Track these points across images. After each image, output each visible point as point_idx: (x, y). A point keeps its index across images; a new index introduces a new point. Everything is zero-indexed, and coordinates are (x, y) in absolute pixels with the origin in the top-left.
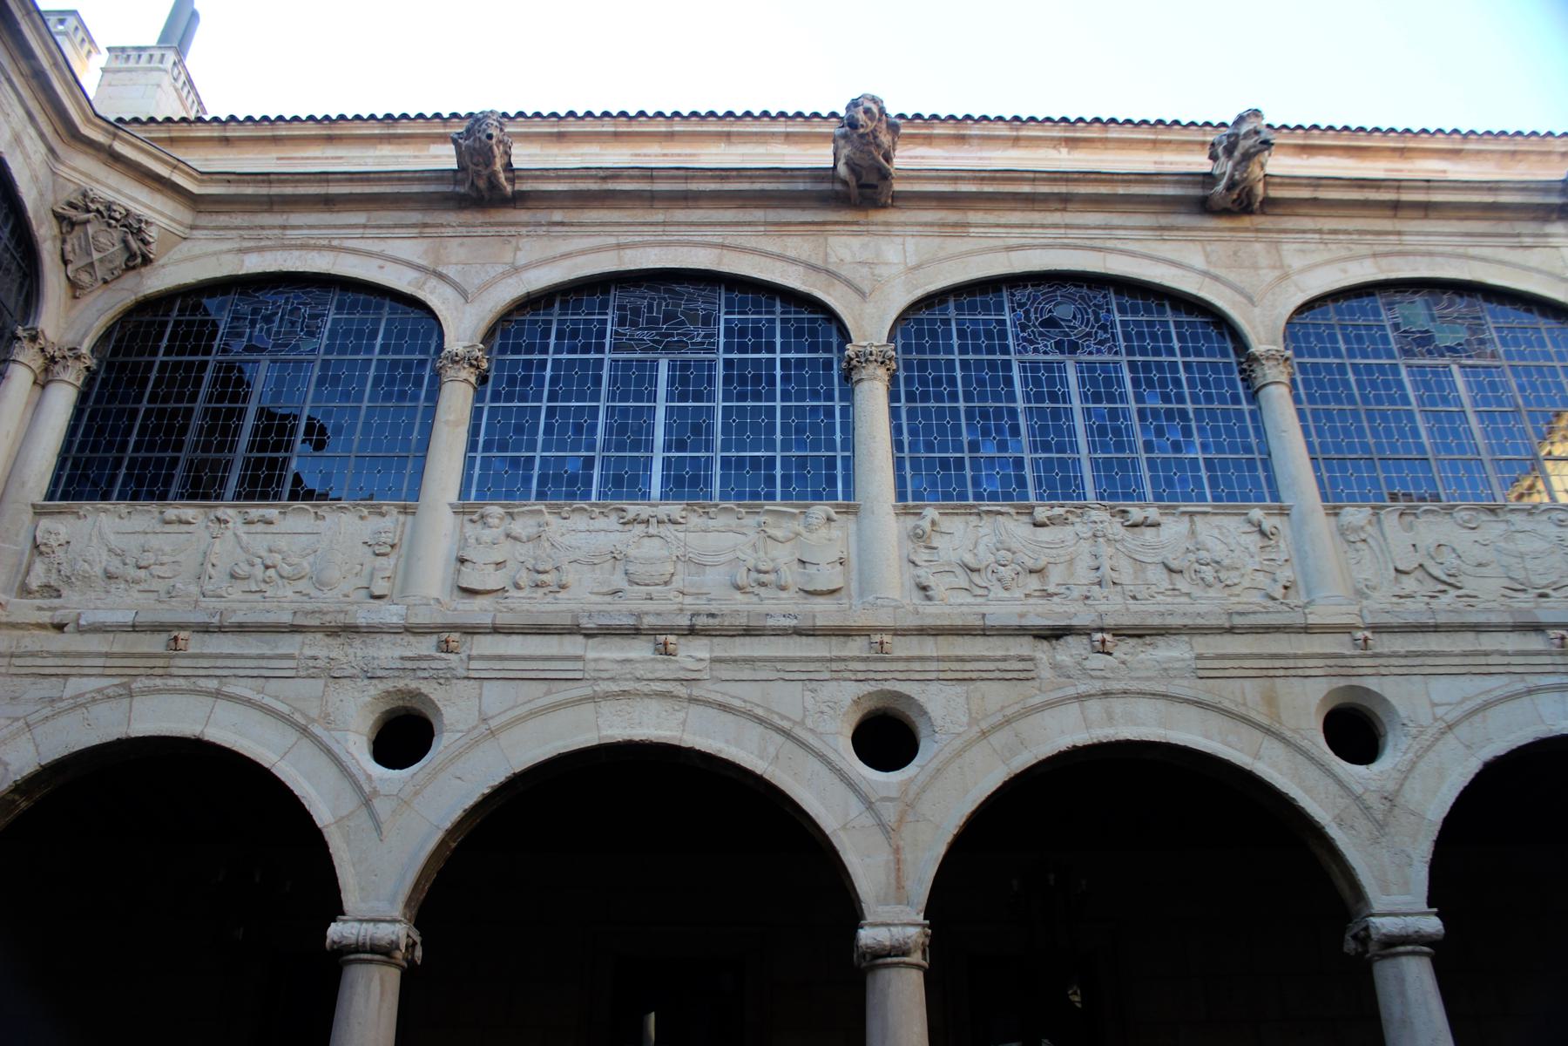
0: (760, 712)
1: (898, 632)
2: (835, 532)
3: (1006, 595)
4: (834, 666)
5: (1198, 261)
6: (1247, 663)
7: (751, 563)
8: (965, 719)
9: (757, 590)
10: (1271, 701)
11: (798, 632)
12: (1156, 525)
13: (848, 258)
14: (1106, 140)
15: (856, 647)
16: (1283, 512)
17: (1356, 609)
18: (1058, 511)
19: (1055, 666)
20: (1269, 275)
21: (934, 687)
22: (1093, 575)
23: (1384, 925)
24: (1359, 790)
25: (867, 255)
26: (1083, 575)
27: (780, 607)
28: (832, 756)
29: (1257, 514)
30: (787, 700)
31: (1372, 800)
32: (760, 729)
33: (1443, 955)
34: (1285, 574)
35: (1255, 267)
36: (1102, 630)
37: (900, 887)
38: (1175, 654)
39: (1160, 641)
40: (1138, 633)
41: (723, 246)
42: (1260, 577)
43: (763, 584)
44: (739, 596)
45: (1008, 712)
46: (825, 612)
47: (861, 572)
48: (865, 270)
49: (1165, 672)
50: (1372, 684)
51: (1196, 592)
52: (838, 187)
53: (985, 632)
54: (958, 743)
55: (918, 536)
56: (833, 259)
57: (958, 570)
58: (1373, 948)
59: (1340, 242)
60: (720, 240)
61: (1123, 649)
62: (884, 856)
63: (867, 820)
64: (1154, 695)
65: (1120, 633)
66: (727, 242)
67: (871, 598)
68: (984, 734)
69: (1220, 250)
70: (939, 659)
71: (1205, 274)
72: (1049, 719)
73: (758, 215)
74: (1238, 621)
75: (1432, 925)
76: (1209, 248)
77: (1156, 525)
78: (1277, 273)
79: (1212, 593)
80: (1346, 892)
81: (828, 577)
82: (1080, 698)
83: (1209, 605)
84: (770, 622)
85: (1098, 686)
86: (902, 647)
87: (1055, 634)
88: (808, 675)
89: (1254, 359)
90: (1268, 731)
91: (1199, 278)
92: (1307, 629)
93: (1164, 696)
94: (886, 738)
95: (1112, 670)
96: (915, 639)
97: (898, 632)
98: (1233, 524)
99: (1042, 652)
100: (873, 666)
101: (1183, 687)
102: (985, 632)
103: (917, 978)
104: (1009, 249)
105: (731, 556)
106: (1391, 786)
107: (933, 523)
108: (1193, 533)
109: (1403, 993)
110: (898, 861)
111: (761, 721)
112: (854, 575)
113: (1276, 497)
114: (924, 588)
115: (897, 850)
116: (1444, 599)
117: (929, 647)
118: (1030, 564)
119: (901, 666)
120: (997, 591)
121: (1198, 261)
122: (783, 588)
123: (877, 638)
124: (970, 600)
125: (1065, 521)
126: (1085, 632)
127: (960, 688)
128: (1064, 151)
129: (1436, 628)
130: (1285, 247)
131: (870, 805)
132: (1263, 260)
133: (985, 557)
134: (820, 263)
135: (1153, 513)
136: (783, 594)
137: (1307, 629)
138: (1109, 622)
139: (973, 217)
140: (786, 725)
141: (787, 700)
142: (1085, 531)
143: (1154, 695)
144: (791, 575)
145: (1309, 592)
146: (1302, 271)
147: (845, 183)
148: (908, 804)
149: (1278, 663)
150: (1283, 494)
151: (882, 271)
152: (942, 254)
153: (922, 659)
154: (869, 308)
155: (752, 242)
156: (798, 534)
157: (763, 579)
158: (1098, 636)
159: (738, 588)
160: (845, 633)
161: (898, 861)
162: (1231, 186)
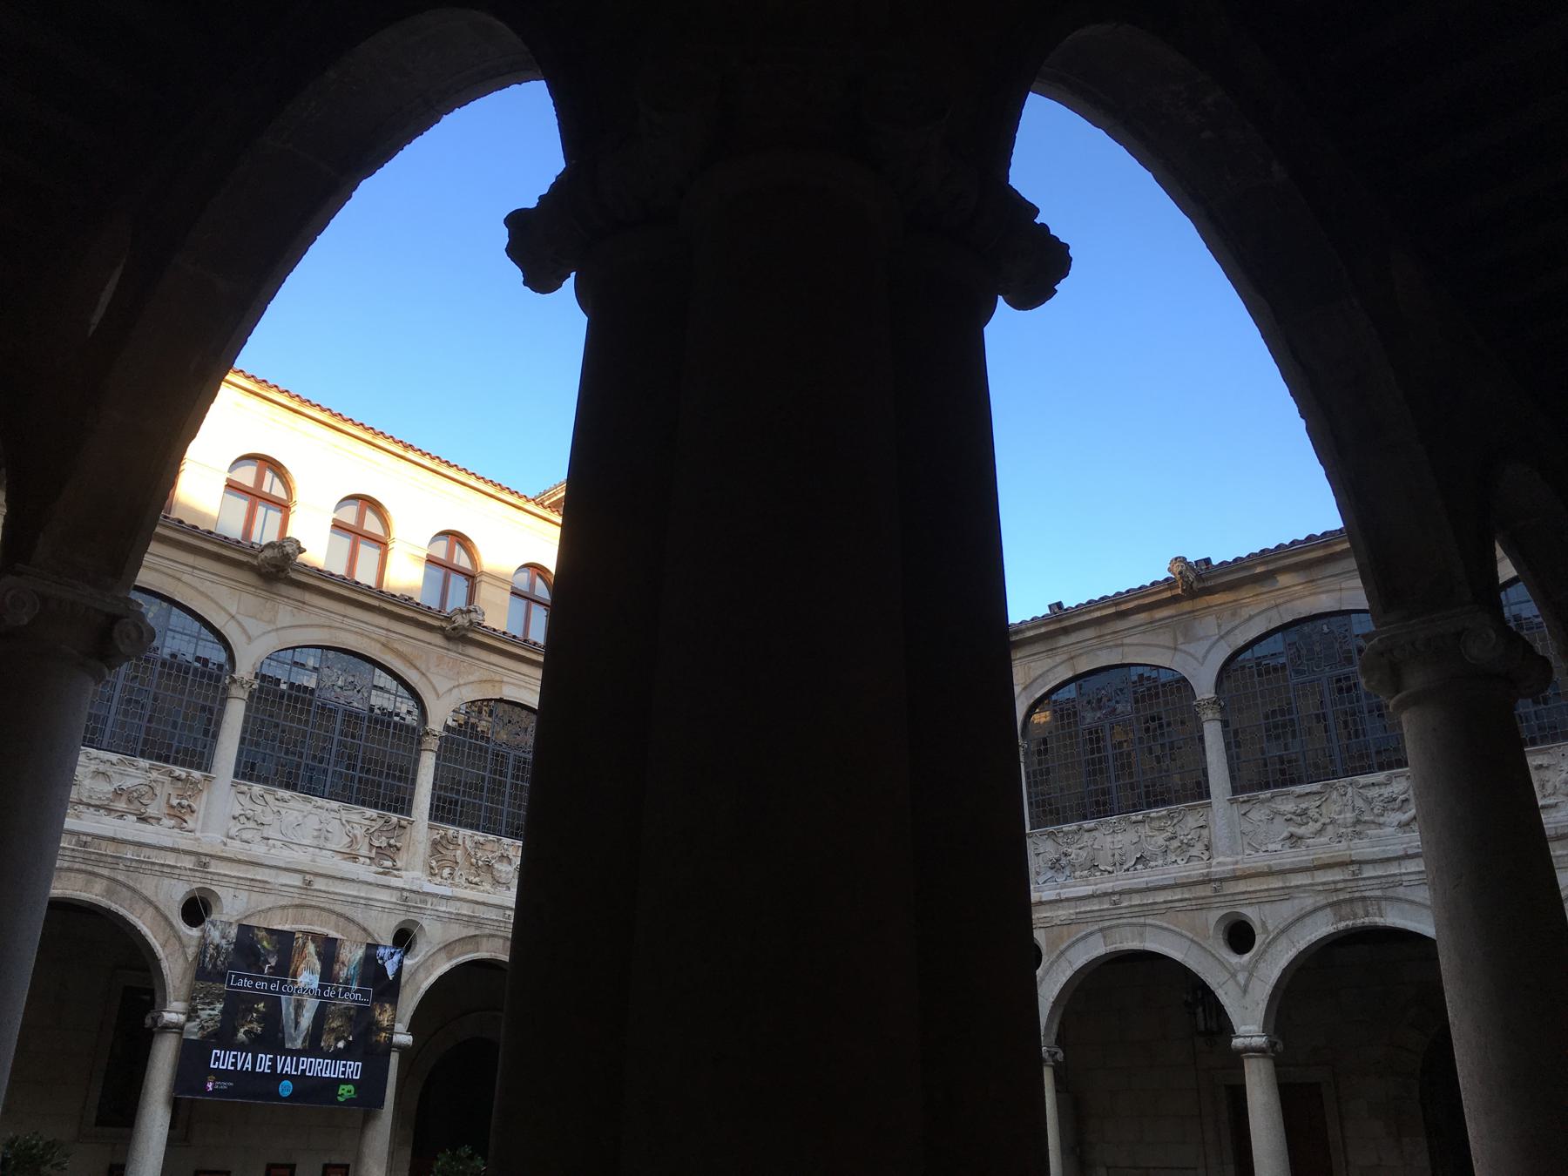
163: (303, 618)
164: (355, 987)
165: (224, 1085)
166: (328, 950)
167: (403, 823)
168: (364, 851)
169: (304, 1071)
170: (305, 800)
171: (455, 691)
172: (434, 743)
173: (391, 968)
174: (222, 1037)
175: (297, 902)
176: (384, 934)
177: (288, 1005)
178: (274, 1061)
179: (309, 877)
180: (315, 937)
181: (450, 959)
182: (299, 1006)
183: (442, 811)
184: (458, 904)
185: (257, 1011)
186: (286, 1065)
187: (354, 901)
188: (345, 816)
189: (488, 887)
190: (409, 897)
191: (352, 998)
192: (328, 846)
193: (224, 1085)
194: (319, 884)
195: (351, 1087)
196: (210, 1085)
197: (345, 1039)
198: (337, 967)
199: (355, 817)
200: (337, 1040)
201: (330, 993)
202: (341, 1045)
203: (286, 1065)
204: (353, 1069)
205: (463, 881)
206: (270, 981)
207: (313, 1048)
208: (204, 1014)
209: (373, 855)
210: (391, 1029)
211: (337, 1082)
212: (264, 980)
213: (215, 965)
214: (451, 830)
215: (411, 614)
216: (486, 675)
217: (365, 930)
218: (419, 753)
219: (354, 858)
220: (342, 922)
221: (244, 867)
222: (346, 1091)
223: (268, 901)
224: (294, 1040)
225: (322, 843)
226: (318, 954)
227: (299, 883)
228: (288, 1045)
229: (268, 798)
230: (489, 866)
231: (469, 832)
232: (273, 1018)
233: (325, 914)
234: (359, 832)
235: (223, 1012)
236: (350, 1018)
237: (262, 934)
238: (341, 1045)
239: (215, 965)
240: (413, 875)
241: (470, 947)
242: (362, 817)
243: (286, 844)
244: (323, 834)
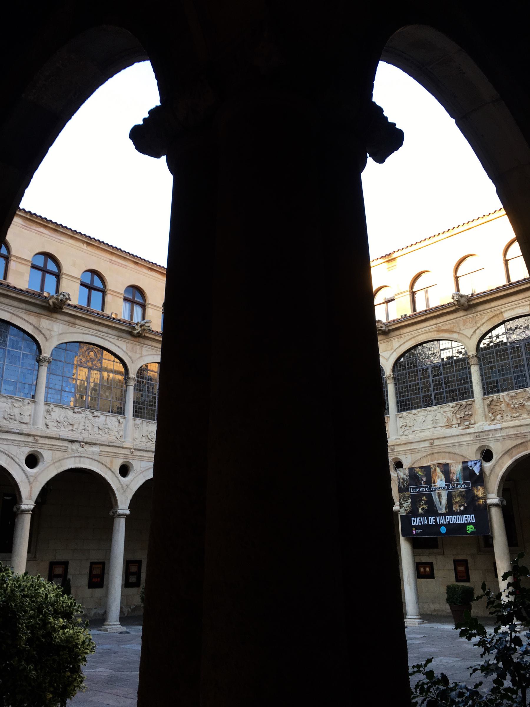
0: (7, 452)
1: (41, 437)
2: (29, 407)
3: (64, 429)
4: (25, 443)
5: (124, 348)
6: (109, 454)
7: (9, 413)
8: (51, 459)
9: (9, 420)
10: (111, 462)
11: (19, 434)
12: (99, 417)
13: (45, 327)
14: (99, 247)
15: (31, 439)
16: (125, 418)
17: (132, 444)
18: (80, 410)
19: (72, 449)
20: (138, 356)
21: (45, 451)
22: (83, 427)
23: (120, 512)
24: (122, 483)
25: (50, 327)
26: (82, 427)
27: (14, 426)
28: (21, 464)
29: (119, 418)
30: (13, 450)
31: (124, 486)
32: (6, 456)
33: (128, 519)
34: (121, 433)
35: (136, 353)
36: (83, 442)
37: (30, 496)
38: (96, 449)
39: (94, 446)
40: (90, 444)
41: (12, 313)
42: (116, 433)
43: (11, 419)
44: (5, 421)
45: (60, 458)
46: (25, 429)
47: (34, 419)
48: (48, 332)
49: (93, 453)
50: (131, 461)
51: (103, 435)
52: (47, 305)
53: (59, 439)
54: (48, 464)
55: (48, 411)
56: (41, 326)
57: (55, 422)
58: (116, 515)
59: (155, 350)
60: (12, 311)
61: (86, 447)
62: (28, 488)
63: (26, 480)
64: (90, 458)
65: (87, 443)
66: (14, 313)
67: (36, 427)
68: (54, 463)
69: (130, 345)
70: (48, 444)
71: (125, 352)
72: (68, 461)
73: (23, 306)
74: (110, 444)
75: (128, 512)
76: (128, 345)
77: (99, 417)
78: (140, 355)
79: (106, 435)
80: (114, 503)
81: (26, 419)
82: (75, 457)
83: (104, 438)
84: (13, 431)
85: (79, 455)
86: (41, 441)
87: (73, 442)
88: (19, 444)
89: (129, 378)
90: (109, 469)
91: (123, 352)
92: (122, 448)
93: (92, 459)
94: (32, 461)
95: (83, 451)
96: (44, 439)
97: (41, 437)
98: (114, 419)
99: (69, 445)
100: (34, 444)
101: (96, 457)
102: (59, 439)
103: (30, 516)
104: (83, 333)
105: (4, 410)
106: (128, 483)
107: (52, 409)
108: (106, 420)
109: (119, 525)
110: (31, 490)
111: (6, 454)
112: (32, 419)
113: (124, 414)
114: (47, 425)
115: (31, 488)
116: (149, 444)
117: (47, 441)
118: (71, 423)
119: (40, 445)
120: (63, 429)
121: (124, 348)
122: (15, 420)
123: (36, 438)
124: (56, 429)
125: (79, 413)
126: (80, 442)
127: (51, 452)
128: (85, 245)
129: (146, 451)
130: (144, 348)
131: (27, 477)
132: (138, 351)
133: (61, 419)
134: (38, 327)
135: (99, 414)
136: (15, 422)
137: (122, 448)
138: (85, 440)
139: (78, 322)
140: (12, 456)
141: (13, 450)
142: (84, 416)
143: (90, 458)
144: (18, 417)
145: (125, 438)
146: (145, 356)
147: (50, 305)
148: (36, 477)
149: (115, 454)
150: (125, 414)
151: (52, 333)
152: (68, 332)
153: (45, 444)
154: (48, 344)
155: (21, 315)
156: (21, 406)
157: (11, 418)
158: (82, 443)
159: (5, 419)
160: (29, 435)
161: (31, 490)
162: (138, 333)
163: (402, 340)
164: (462, 482)
165: (419, 531)
166: (446, 469)
167: (469, 403)
168: (455, 422)
169: (449, 522)
170: (424, 410)
171: (478, 331)
172: (473, 361)
173: (477, 470)
174: (413, 512)
175: (430, 453)
176: (472, 454)
177: (435, 495)
178: (435, 519)
179: (431, 441)
180: (439, 465)
181: (512, 458)
182: (439, 495)
183: (489, 388)
184: (507, 430)
185: (424, 500)
186: (441, 520)
187: (453, 445)
188: (442, 410)
189: (525, 416)
190: (478, 435)
191: (461, 488)
192: (439, 425)
193: (419, 531)
194: (437, 443)
195: (472, 526)
196: (414, 532)
197: (463, 505)
198: (451, 475)
199: (447, 409)
200: (460, 506)
201: (451, 487)
202: (462, 508)
203: (441, 520)
204: (470, 518)
205: (509, 418)
206: (425, 487)
207: (450, 511)
208: (405, 505)
209: (459, 422)
210: (485, 498)
211: (465, 525)
212: (423, 487)
213: (404, 486)
214: (495, 396)
215: (424, 317)
216: (492, 314)
217: (462, 456)
218: (469, 368)
219: (451, 426)
220: (451, 455)
221: (406, 446)
222: (470, 528)
223: (419, 456)
224: (441, 509)
225: (435, 425)
226: (442, 472)
227: (428, 445)
228: (440, 512)
229: (410, 415)
230: (523, 406)
231: (505, 393)
232: (430, 502)
233: (443, 454)
234: (450, 415)
235: (411, 503)
236: (463, 496)
237: (418, 469)
238: (462, 508)
239: (404, 486)
240: (481, 424)
241: (521, 449)
242: (449, 408)
243: (421, 431)
244: (435, 421)
